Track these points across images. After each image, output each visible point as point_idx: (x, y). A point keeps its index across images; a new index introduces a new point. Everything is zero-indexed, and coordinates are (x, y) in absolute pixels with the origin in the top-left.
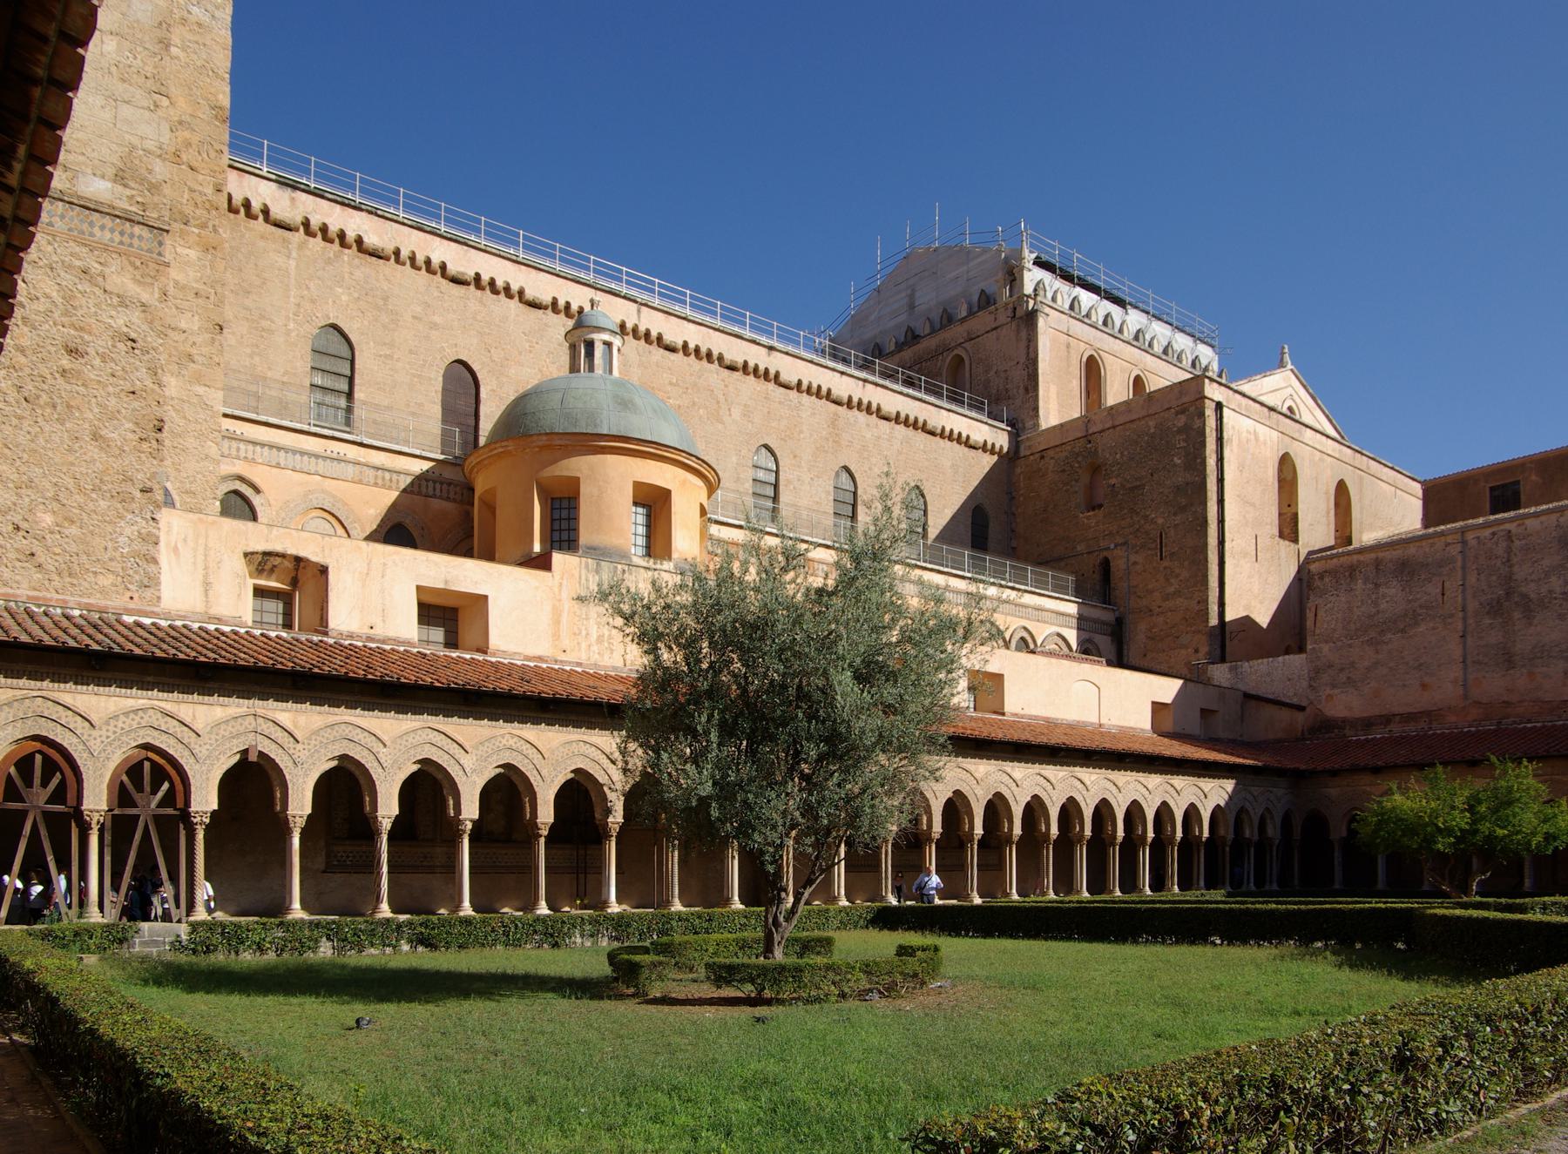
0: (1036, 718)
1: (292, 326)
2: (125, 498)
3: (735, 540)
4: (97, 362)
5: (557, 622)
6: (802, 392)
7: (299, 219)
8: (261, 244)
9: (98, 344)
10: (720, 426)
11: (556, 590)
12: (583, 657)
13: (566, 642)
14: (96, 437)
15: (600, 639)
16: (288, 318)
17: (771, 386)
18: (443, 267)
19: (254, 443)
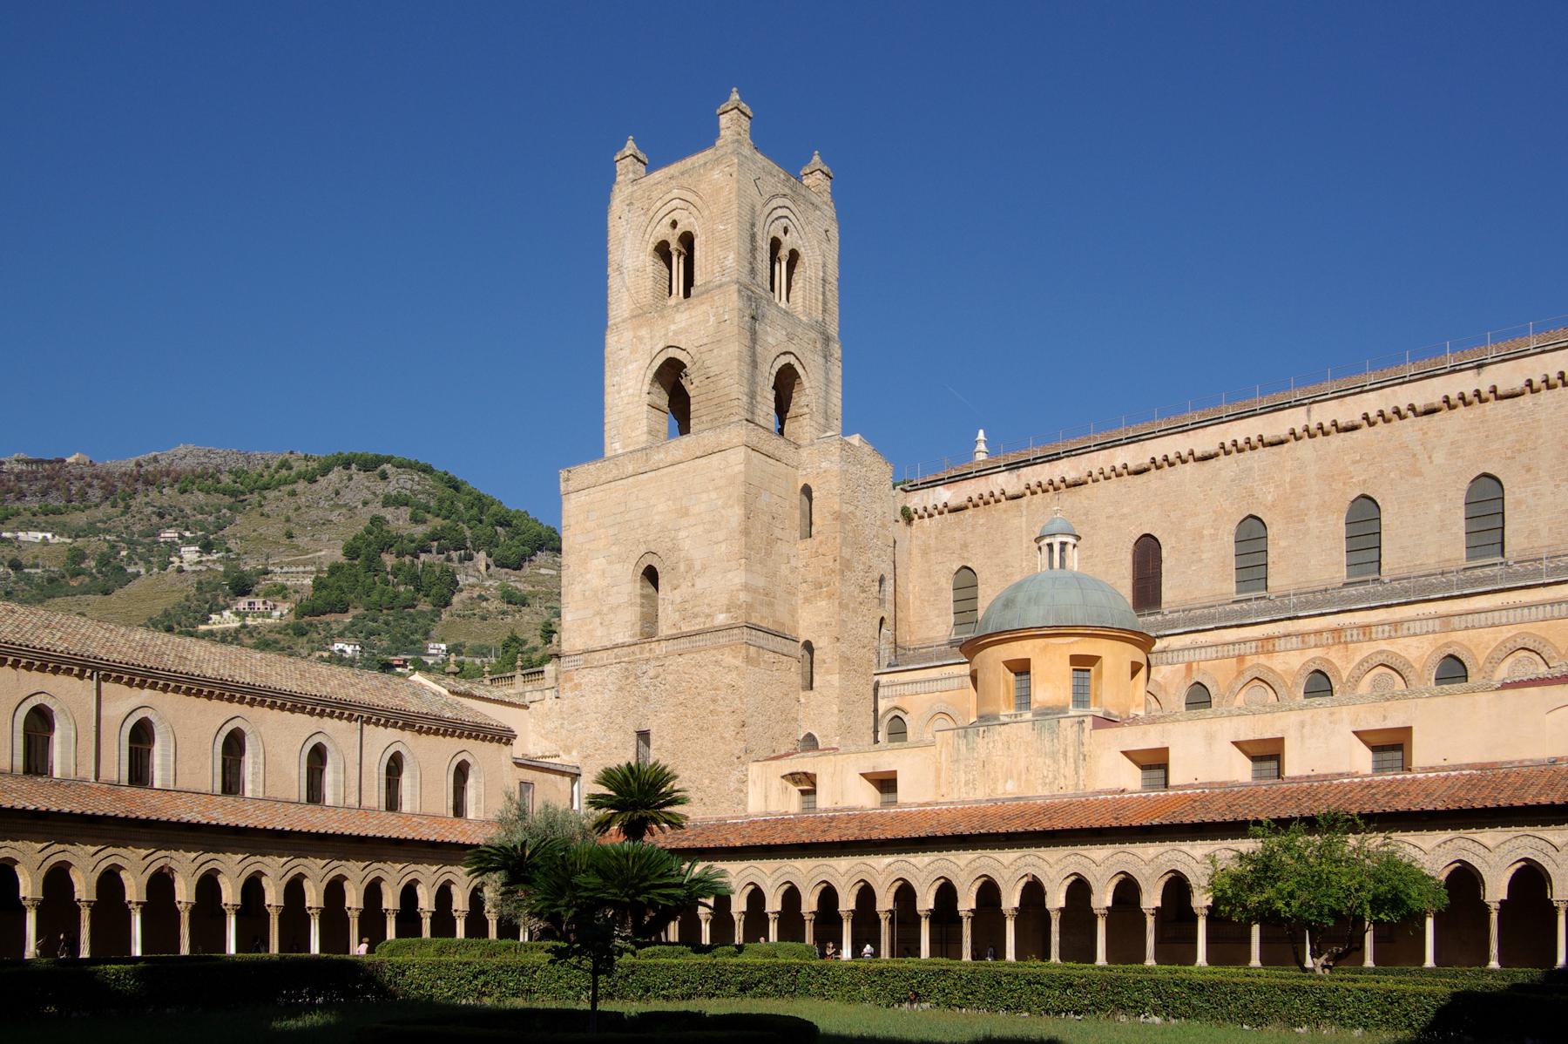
0: (1211, 785)
1: (1024, 564)
2: (731, 764)
3: (1271, 634)
4: (721, 703)
5: (938, 777)
6: (1538, 391)
8: (1004, 516)
9: (722, 694)
10: (1417, 480)
11: (937, 756)
12: (954, 797)
13: (944, 790)
14: (722, 738)
15: (967, 783)
16: (1022, 560)
17: (1492, 405)
19: (904, 684)
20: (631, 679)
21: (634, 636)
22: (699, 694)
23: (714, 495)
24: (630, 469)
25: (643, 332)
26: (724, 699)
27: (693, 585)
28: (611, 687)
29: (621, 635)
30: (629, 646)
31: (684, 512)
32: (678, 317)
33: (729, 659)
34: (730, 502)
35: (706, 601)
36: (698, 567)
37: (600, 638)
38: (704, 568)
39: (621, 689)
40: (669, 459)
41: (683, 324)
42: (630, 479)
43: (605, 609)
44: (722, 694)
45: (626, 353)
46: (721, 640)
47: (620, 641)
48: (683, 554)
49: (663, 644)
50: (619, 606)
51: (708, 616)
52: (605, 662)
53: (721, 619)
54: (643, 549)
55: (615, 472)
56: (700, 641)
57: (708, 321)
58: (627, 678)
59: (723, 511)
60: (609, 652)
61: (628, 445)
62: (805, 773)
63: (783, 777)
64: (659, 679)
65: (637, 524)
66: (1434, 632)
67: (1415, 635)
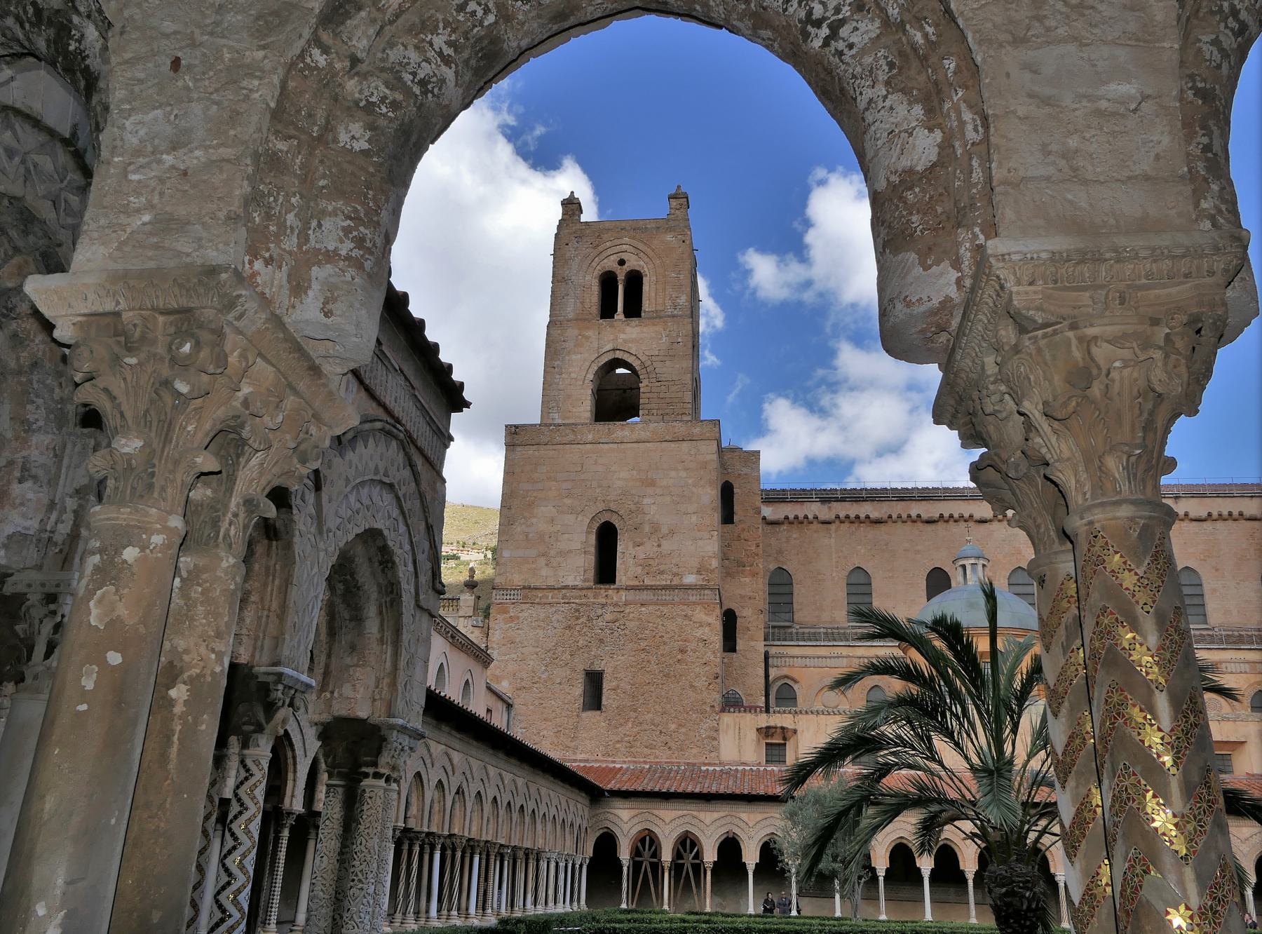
2: (703, 712)
7: (833, 517)
14: (692, 686)
18: (919, 516)
20: (583, 620)
21: (584, 581)
22: (665, 643)
23: (683, 474)
24: (590, 437)
25: (590, 333)
26: (694, 651)
27: (659, 546)
28: (556, 625)
29: (571, 578)
30: (581, 589)
31: (652, 483)
32: (628, 329)
33: (699, 615)
34: (702, 483)
35: (674, 562)
36: (665, 530)
37: (545, 576)
38: (672, 532)
39: (569, 627)
40: (635, 437)
41: (634, 336)
42: (588, 446)
43: (552, 553)
44: (692, 645)
45: (570, 345)
46: (691, 598)
47: (571, 584)
48: (647, 517)
49: (623, 594)
50: (570, 551)
51: (675, 575)
52: (550, 600)
53: (690, 579)
54: (601, 507)
55: (571, 437)
56: (666, 596)
57: (661, 339)
58: (578, 619)
59: (694, 489)
60: (556, 592)
61: (568, 418)
62: (783, 728)
63: (758, 730)
65: (594, 484)
66: (1246, 673)
67: (1232, 673)
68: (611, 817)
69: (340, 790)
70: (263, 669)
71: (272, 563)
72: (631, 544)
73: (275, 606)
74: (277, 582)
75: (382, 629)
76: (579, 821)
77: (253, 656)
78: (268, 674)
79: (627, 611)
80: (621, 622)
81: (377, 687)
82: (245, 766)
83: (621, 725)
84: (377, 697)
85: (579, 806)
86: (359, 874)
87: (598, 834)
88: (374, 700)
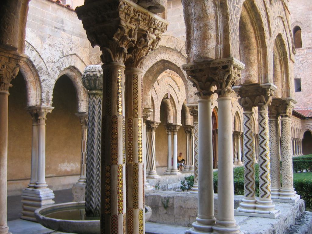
64: (304, 62)
68: (309, 126)
69: (274, 122)
70: (263, 85)
71: (259, 49)
72: (306, 33)
73: (262, 64)
74: (261, 55)
75: (281, 69)
76: (298, 128)
77: (259, 80)
78: (265, 86)
79: (307, 57)
80: (306, 61)
81: (282, 88)
82: (261, 116)
83: (309, 95)
84: (283, 91)
85: (298, 123)
86: (285, 147)
87: (305, 131)
88: (282, 92)
